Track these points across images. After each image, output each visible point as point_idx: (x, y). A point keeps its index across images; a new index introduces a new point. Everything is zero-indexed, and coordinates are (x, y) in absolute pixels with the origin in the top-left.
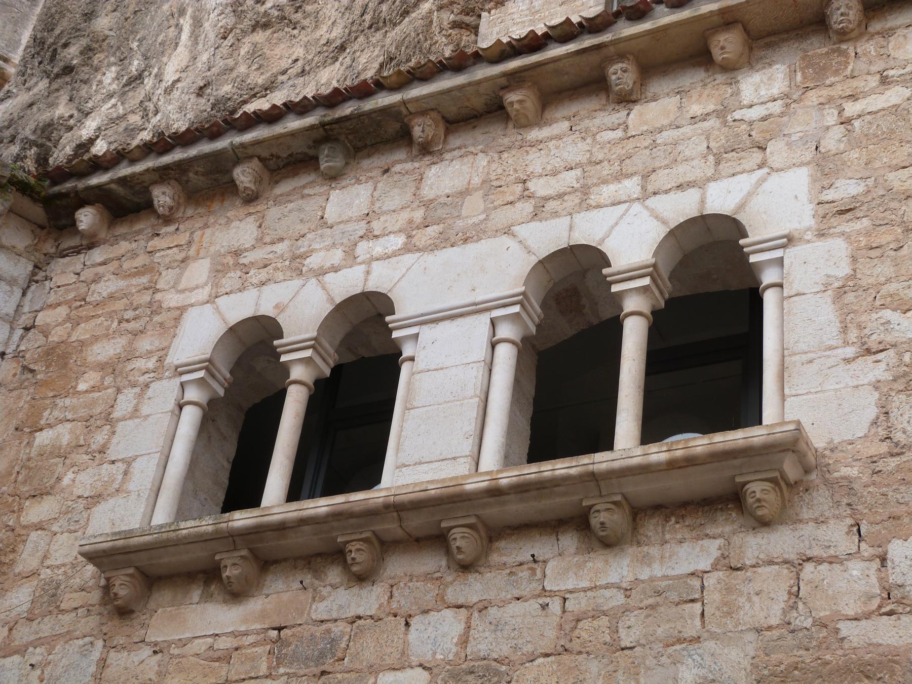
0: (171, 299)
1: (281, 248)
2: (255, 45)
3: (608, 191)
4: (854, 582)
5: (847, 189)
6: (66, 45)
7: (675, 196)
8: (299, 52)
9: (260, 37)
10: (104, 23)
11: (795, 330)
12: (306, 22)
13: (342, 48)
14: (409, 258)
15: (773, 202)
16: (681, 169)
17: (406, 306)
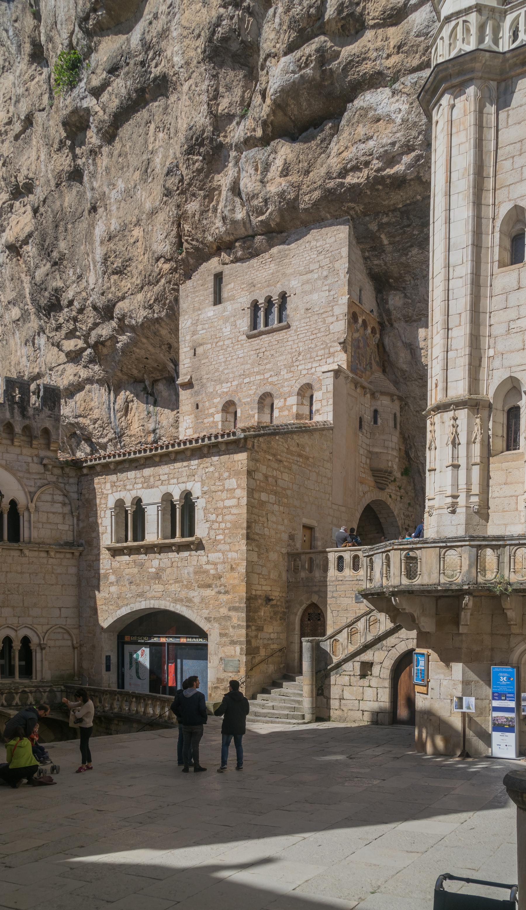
0: (105, 492)
1: (122, 483)
2: (115, 280)
3: (172, 481)
4: (204, 559)
5: (206, 488)
6: (52, 251)
7: (182, 484)
8: (129, 286)
9: (116, 277)
10: (62, 245)
11: (199, 515)
12: (129, 274)
13: (142, 288)
14: (143, 490)
15: (196, 490)
16: (183, 478)
17: (144, 502)
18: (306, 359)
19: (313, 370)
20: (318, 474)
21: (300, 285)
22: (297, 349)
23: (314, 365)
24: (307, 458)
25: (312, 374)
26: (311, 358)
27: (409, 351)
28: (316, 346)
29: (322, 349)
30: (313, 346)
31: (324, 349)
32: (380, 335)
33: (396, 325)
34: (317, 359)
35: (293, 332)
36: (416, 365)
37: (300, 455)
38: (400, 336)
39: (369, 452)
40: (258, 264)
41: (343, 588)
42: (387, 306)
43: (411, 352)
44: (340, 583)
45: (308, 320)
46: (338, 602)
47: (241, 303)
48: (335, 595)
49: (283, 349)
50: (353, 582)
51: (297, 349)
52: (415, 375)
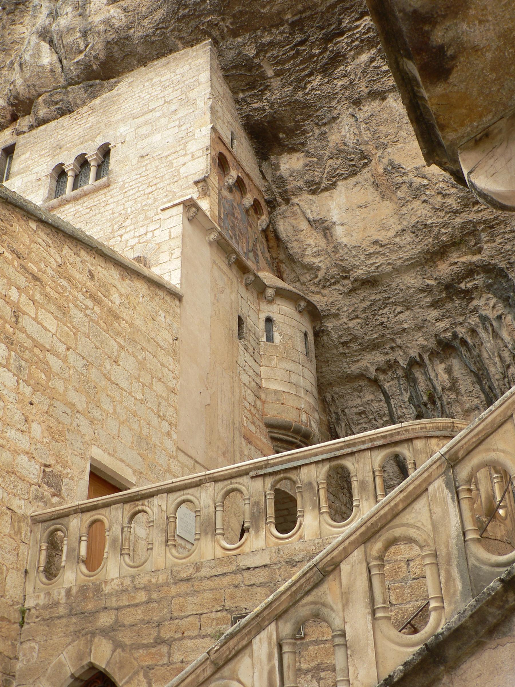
18: (137, 222)
19: (150, 235)
20: (142, 364)
21: (133, 129)
22: (123, 212)
23: (151, 228)
25: (146, 242)
26: (146, 219)
27: (321, 235)
28: (155, 200)
30: (150, 201)
32: (270, 219)
33: (295, 200)
35: (118, 190)
38: (304, 213)
40: (71, 121)
41: (192, 605)
44: (184, 587)
45: (144, 169)
46: (177, 657)
47: (37, 173)
48: (166, 634)
49: (99, 216)
50: (226, 581)
51: (123, 212)
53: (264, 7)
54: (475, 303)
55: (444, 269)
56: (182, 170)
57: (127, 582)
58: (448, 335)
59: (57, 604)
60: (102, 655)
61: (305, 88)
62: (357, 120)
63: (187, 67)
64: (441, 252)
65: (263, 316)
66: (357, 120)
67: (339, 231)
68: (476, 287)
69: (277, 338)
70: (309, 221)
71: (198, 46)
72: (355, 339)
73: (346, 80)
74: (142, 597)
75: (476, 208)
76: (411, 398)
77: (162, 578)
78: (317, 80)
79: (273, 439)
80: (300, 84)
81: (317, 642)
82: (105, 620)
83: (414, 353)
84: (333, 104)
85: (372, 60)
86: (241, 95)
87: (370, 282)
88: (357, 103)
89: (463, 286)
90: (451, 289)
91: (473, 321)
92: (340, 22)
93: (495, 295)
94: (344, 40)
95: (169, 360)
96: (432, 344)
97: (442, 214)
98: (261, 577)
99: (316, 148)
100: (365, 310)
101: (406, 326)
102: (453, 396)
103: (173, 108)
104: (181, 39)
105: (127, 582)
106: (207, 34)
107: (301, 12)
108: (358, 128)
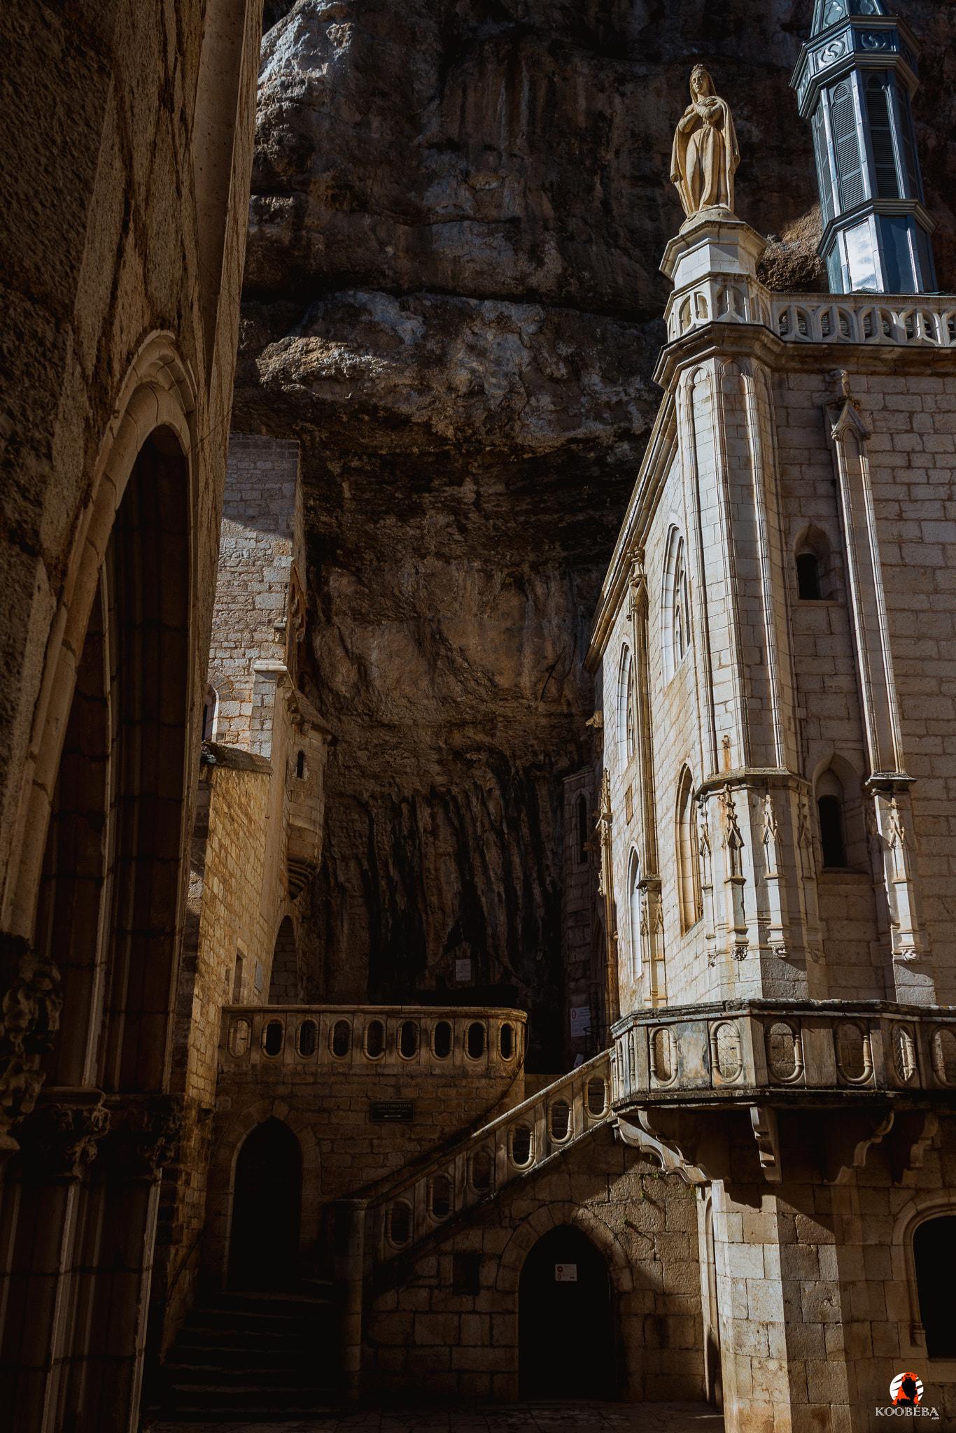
24: (250, 820)
27: (356, 666)
29: (237, 631)
31: (242, 631)
33: (336, 619)
34: (225, 644)
36: (367, 691)
37: (246, 814)
39: (289, 825)
42: (326, 589)
43: (359, 669)
52: (360, 708)
53: (364, 437)
54: (473, 771)
55: (457, 739)
56: (258, 599)
57: (299, 1068)
58: (443, 789)
59: (246, 1074)
60: (281, 1111)
61: (376, 522)
62: (417, 573)
63: (269, 465)
64: (462, 725)
65: (296, 749)
66: (417, 573)
67: (375, 672)
68: (479, 760)
69: (306, 773)
70: (347, 650)
71: (284, 441)
72: (359, 766)
73: (418, 531)
74: (310, 1079)
75: (501, 703)
76: (393, 831)
77: (325, 1069)
78: (391, 520)
79: (290, 871)
80: (375, 517)
81: (421, 1125)
82: (282, 1090)
83: (407, 793)
84: (399, 547)
85: (448, 525)
86: (311, 502)
87: (390, 727)
88: (423, 557)
89: (468, 756)
90: (458, 754)
91: (467, 785)
92: (431, 480)
93: (493, 771)
94: (427, 498)
95: (263, 839)
96: (424, 791)
97: (471, 697)
98: (392, 1081)
99: (370, 580)
100: (376, 746)
101: (408, 770)
102: (431, 839)
103: (251, 512)
104: (267, 425)
105: (299, 1068)
106: (298, 434)
107: (396, 454)
108: (418, 583)
